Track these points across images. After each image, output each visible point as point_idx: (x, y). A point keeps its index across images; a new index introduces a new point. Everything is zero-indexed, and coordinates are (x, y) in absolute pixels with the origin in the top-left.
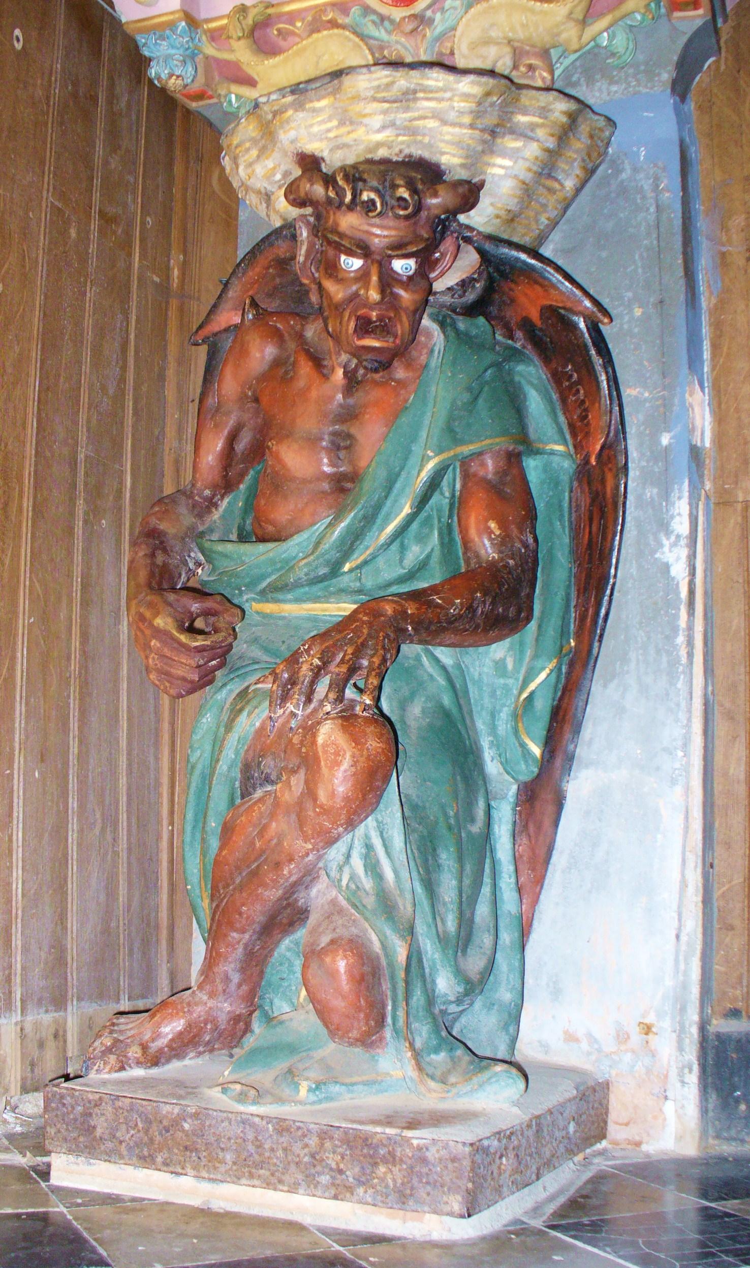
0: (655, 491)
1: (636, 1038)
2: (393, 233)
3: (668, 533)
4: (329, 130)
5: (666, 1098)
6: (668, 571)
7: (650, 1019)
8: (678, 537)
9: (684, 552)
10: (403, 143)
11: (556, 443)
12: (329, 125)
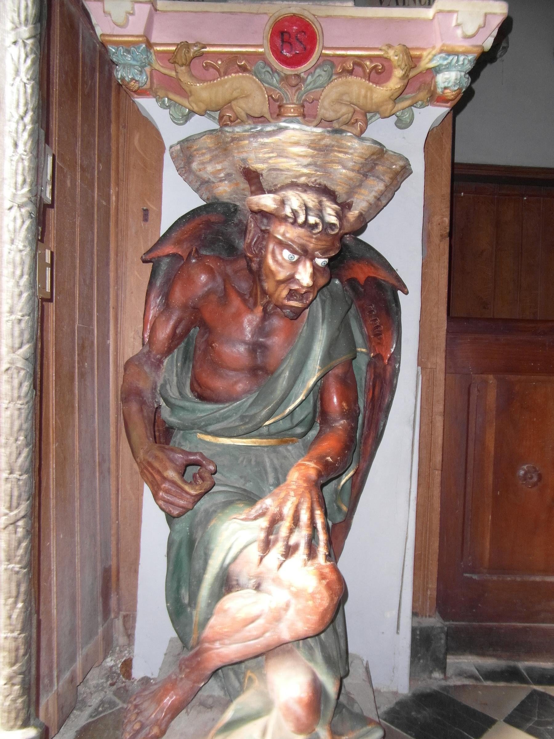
2: (324, 243)
4: (270, 158)
10: (318, 176)
12: (271, 155)
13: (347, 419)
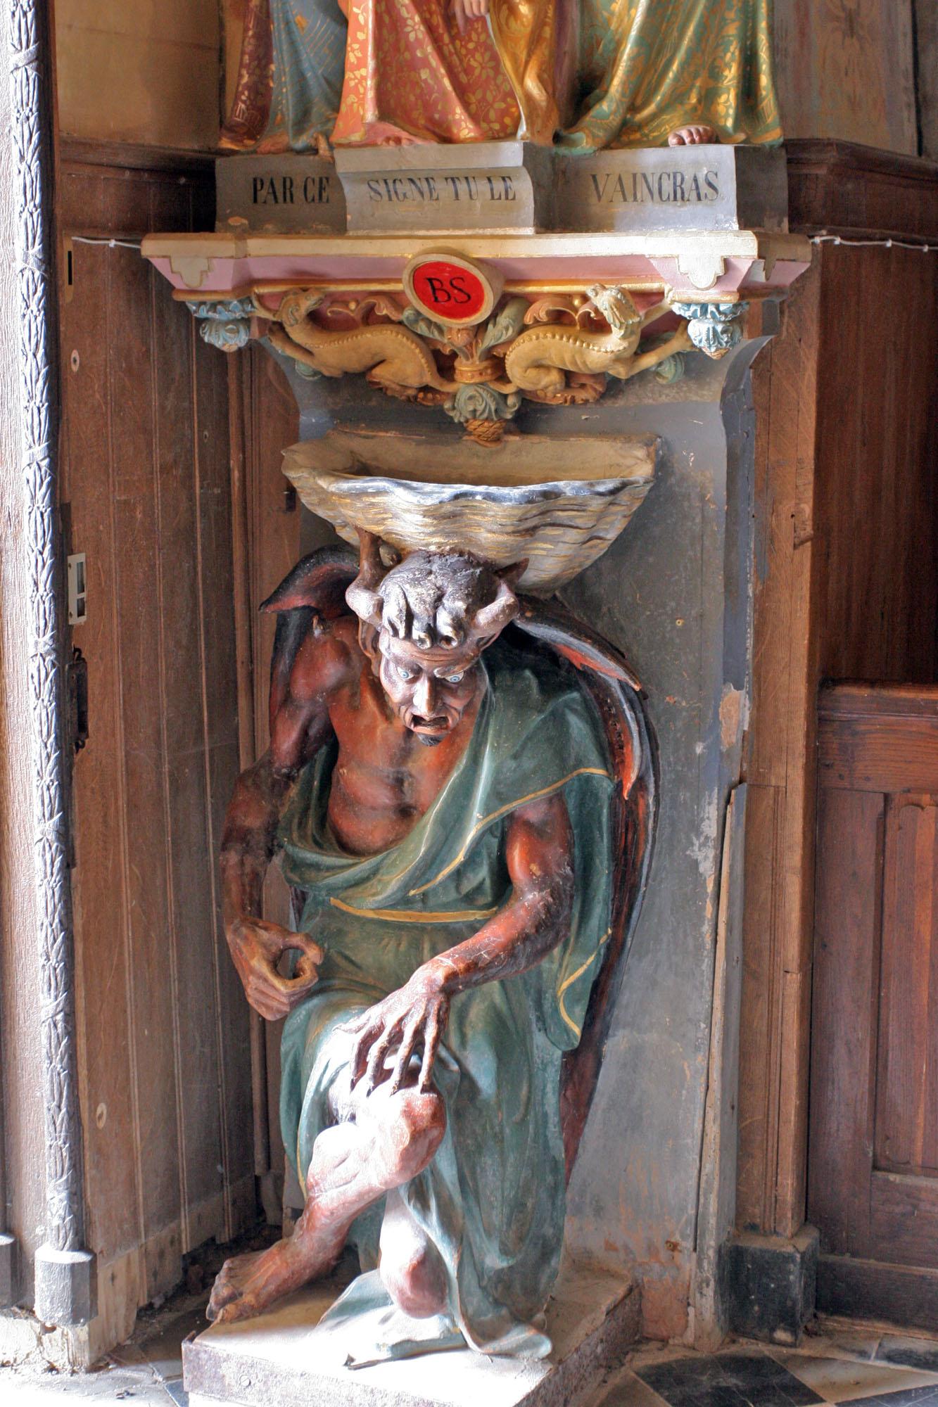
0: (688, 794)
1: (664, 1254)
3: (698, 833)
5: (689, 1304)
6: (697, 868)
7: (677, 1238)
8: (707, 838)
9: (711, 853)
11: (596, 767)
13: (541, 890)
